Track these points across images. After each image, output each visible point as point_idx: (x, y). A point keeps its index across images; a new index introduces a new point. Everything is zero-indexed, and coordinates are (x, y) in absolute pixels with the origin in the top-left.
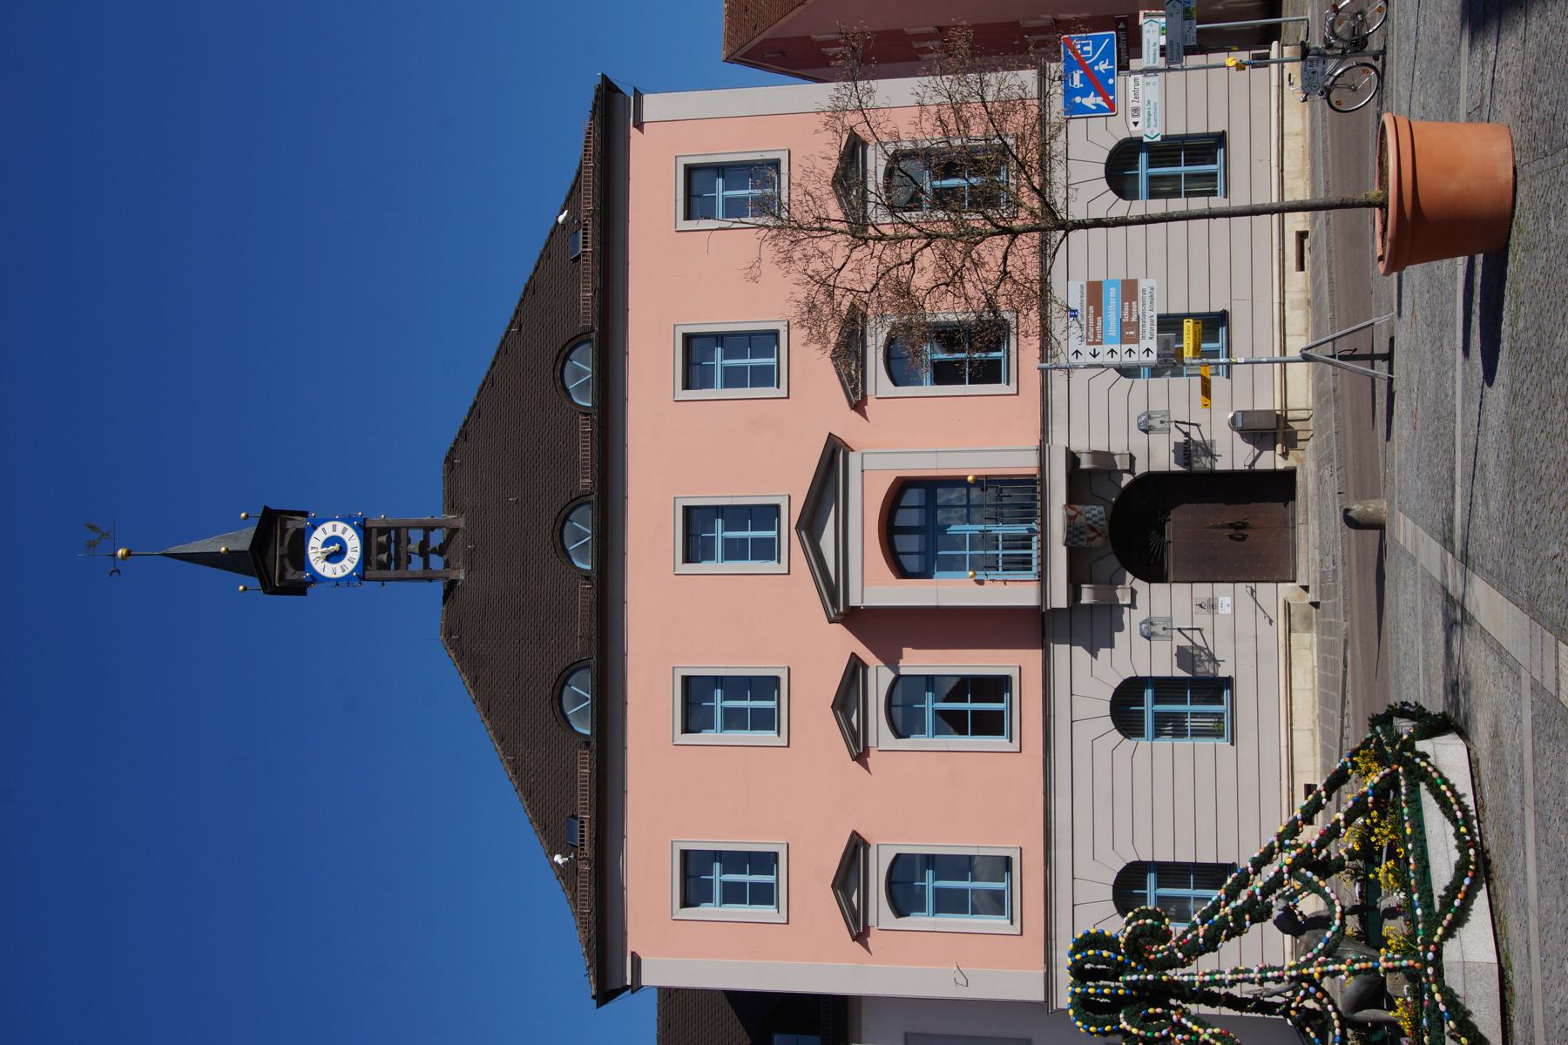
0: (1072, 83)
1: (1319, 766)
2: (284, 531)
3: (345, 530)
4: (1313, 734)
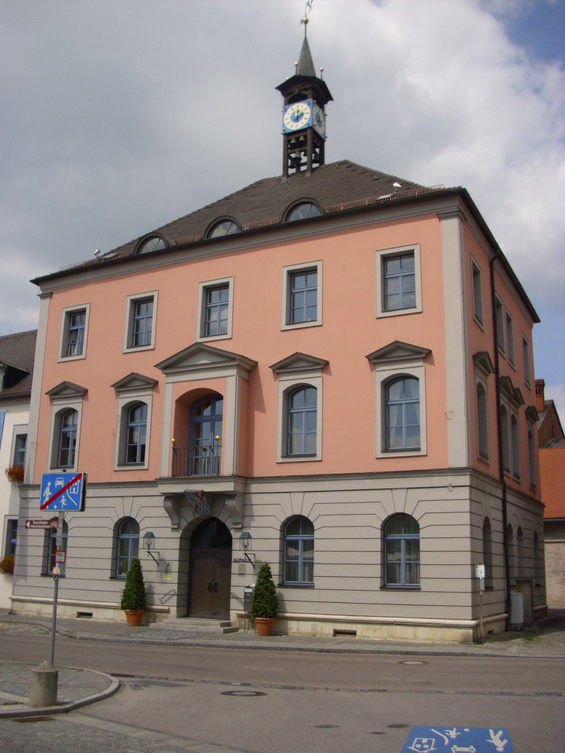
0: (58, 480)
1: (99, 620)
2: (306, 90)
3: (306, 119)
4: (112, 619)
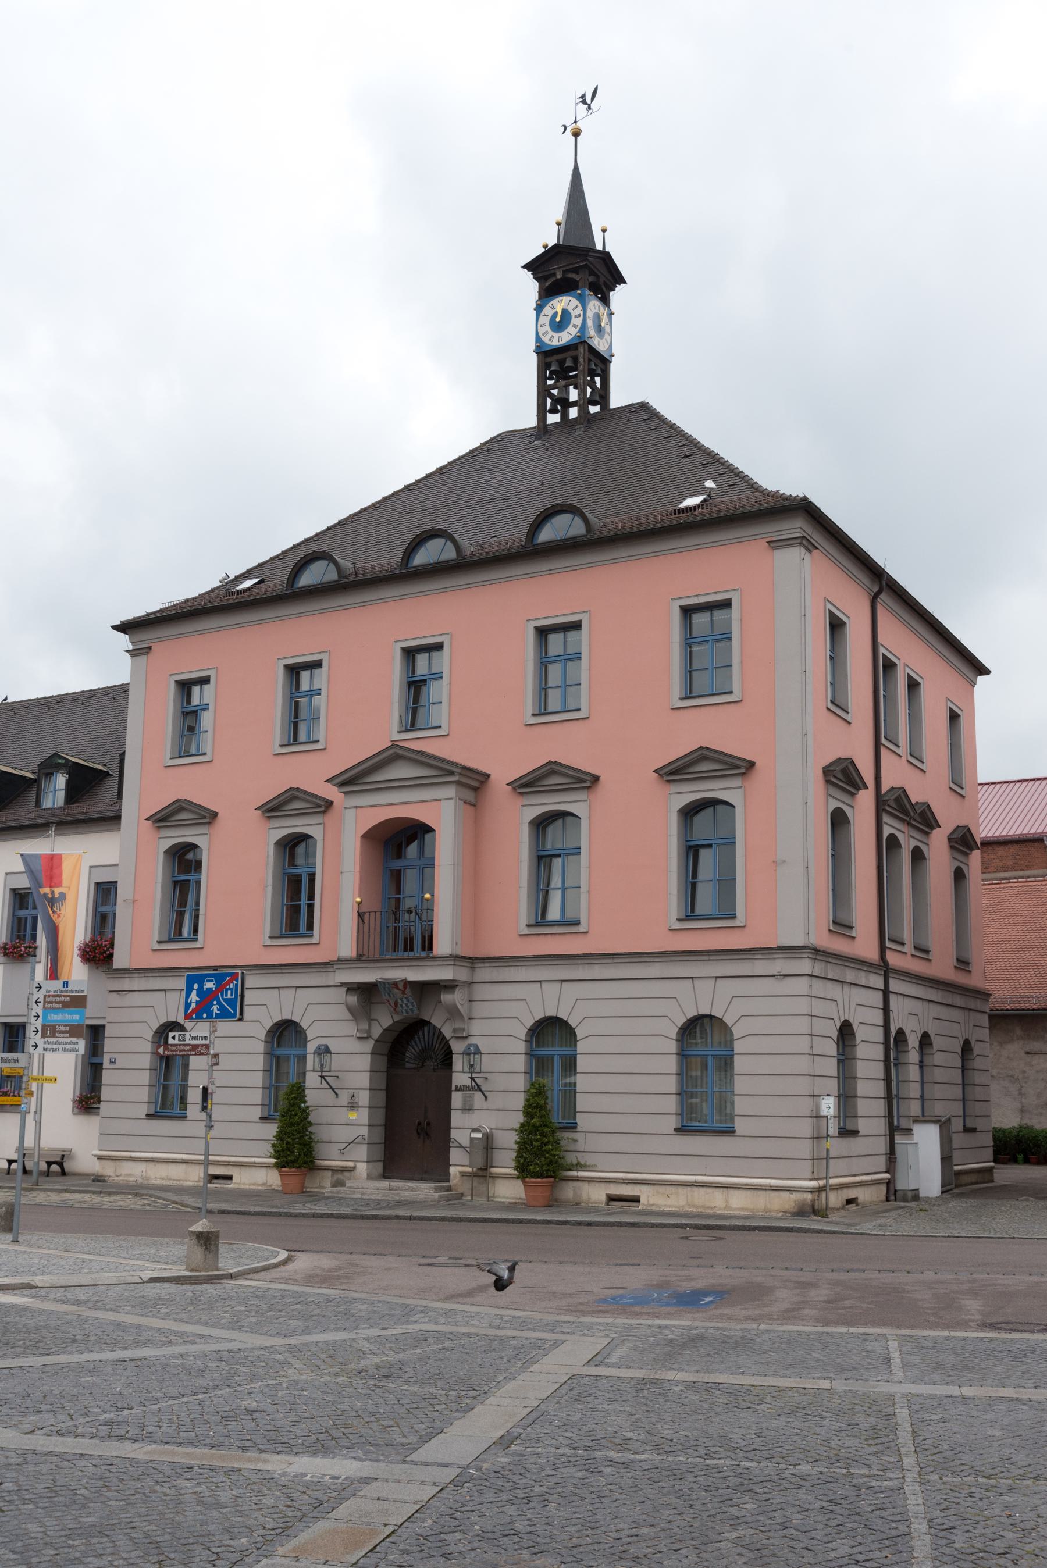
0: (208, 981)
1: (242, 1187)
3: (575, 326)
4: (264, 1184)
